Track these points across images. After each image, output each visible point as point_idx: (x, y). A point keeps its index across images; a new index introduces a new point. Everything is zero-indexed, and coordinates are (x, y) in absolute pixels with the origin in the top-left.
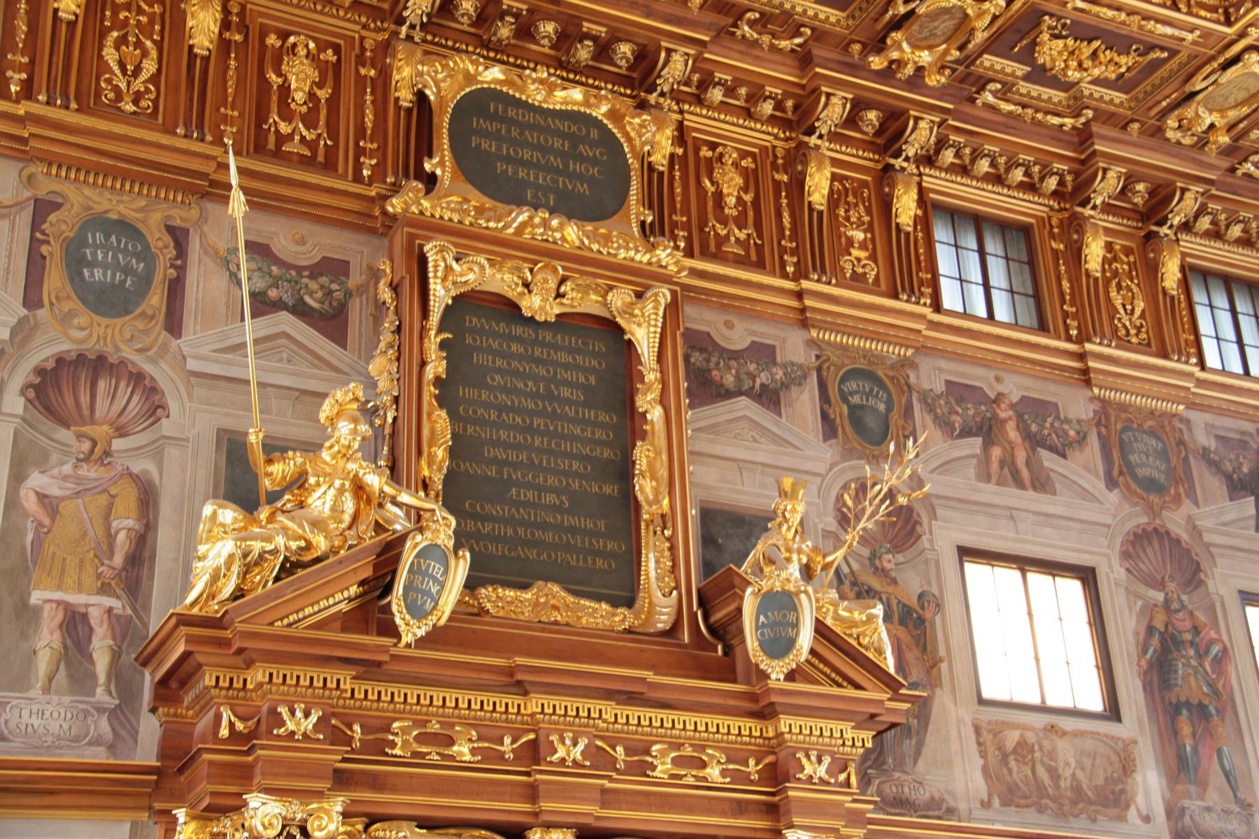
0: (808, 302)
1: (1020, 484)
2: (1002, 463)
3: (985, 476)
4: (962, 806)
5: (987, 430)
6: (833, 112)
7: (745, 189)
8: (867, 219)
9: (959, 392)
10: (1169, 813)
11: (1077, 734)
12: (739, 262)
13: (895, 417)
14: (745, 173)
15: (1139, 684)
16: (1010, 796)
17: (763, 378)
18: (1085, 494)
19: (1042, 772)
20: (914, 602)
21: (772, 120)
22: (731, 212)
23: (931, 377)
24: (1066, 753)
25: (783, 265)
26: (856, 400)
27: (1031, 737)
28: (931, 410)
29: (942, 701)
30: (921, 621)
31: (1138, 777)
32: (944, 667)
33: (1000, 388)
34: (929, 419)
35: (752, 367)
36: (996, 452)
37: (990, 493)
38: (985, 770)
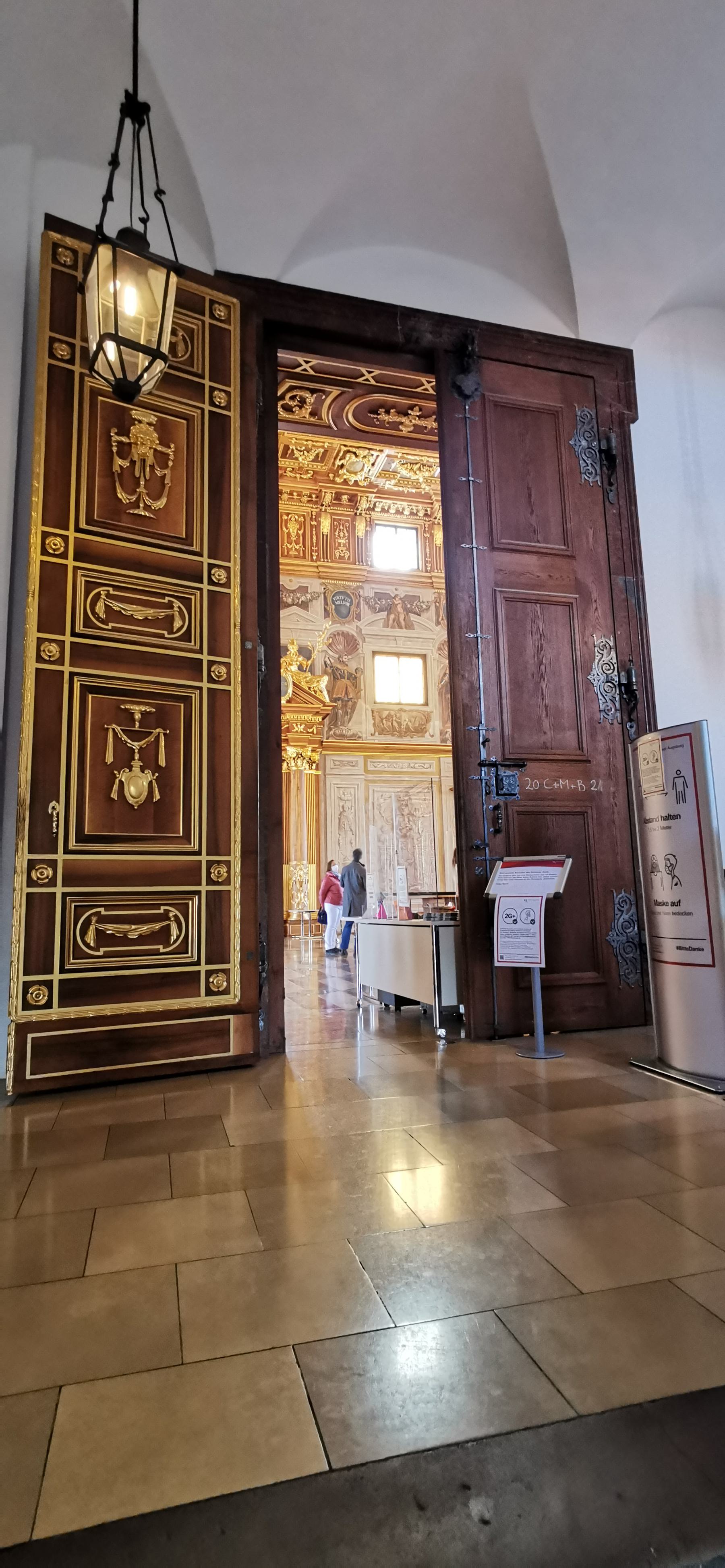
0: (321, 569)
1: (401, 627)
2: (394, 621)
3: (386, 625)
4: (364, 736)
5: (389, 609)
6: (328, 498)
7: (300, 529)
8: (347, 534)
9: (379, 596)
10: (441, 734)
11: (410, 711)
12: (296, 557)
13: (353, 608)
14: (300, 523)
15: (437, 693)
16: (382, 732)
17: (303, 598)
18: (426, 628)
19: (395, 724)
20: (354, 672)
21: (309, 501)
22: (293, 538)
23: (368, 591)
24: (405, 717)
25: (312, 556)
26: (338, 603)
27: (392, 713)
28: (367, 603)
29: (361, 703)
30: (356, 678)
31: (431, 723)
32: (363, 692)
33: (396, 593)
34: (366, 607)
35: (299, 595)
36: (392, 616)
37: (388, 631)
38: (374, 724)
